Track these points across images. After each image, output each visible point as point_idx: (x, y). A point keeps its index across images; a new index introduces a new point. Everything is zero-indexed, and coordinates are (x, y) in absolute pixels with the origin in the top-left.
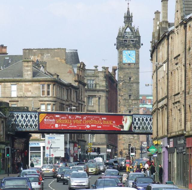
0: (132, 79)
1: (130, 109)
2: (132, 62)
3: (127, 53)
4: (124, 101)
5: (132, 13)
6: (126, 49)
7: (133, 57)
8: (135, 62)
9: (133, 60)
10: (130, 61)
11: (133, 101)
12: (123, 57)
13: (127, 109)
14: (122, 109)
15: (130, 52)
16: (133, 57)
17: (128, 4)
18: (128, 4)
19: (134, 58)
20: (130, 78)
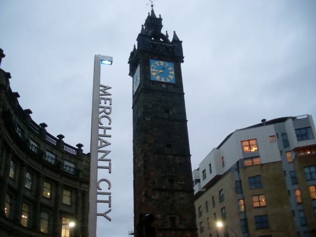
0: (171, 113)
1: (171, 174)
2: (168, 81)
3: (158, 65)
4: (156, 156)
5: (160, 15)
6: (155, 58)
7: (171, 73)
8: (174, 82)
9: (171, 78)
10: (165, 79)
11: (177, 158)
12: (151, 70)
13: (163, 175)
14: (152, 174)
15: (165, 64)
16: (171, 73)
17: (152, 6)
18: (152, 6)
19: (172, 75)
20: (167, 111)
